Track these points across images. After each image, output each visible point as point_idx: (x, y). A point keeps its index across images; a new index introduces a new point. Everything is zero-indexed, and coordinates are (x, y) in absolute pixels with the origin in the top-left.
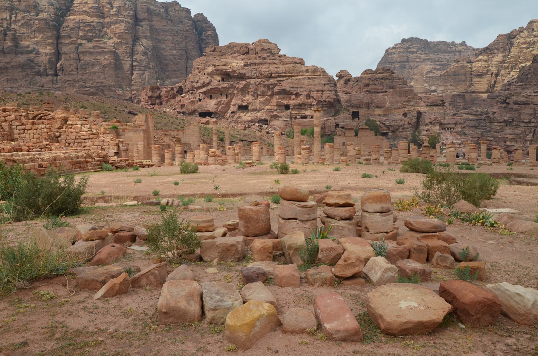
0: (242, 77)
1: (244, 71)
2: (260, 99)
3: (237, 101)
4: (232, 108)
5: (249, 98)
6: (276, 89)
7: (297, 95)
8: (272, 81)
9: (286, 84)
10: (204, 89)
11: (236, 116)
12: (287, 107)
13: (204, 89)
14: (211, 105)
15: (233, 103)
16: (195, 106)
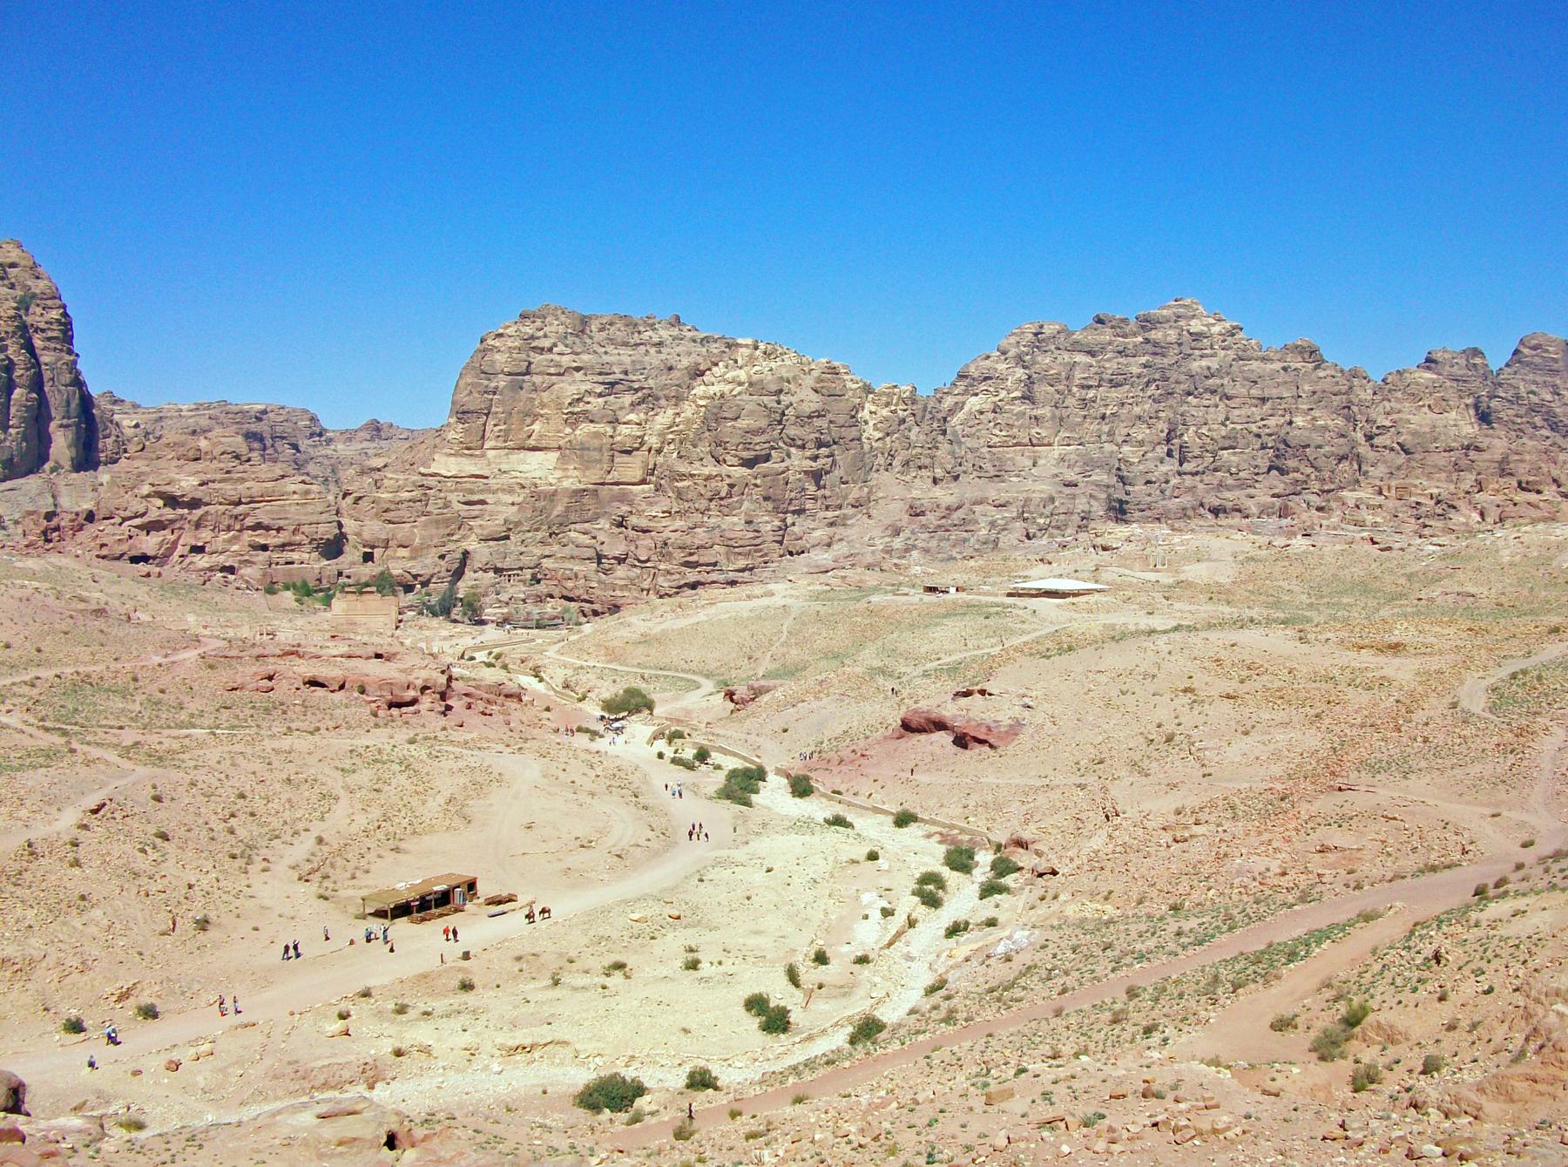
0: (195, 504)
1: (198, 495)
2: (224, 536)
3: (188, 539)
4: (180, 550)
5: (205, 535)
6: (249, 522)
7: (279, 529)
8: (241, 508)
9: (263, 514)
10: (138, 521)
11: (188, 560)
12: (265, 548)
13: (138, 521)
14: (150, 543)
15: (181, 542)
16: (124, 547)
